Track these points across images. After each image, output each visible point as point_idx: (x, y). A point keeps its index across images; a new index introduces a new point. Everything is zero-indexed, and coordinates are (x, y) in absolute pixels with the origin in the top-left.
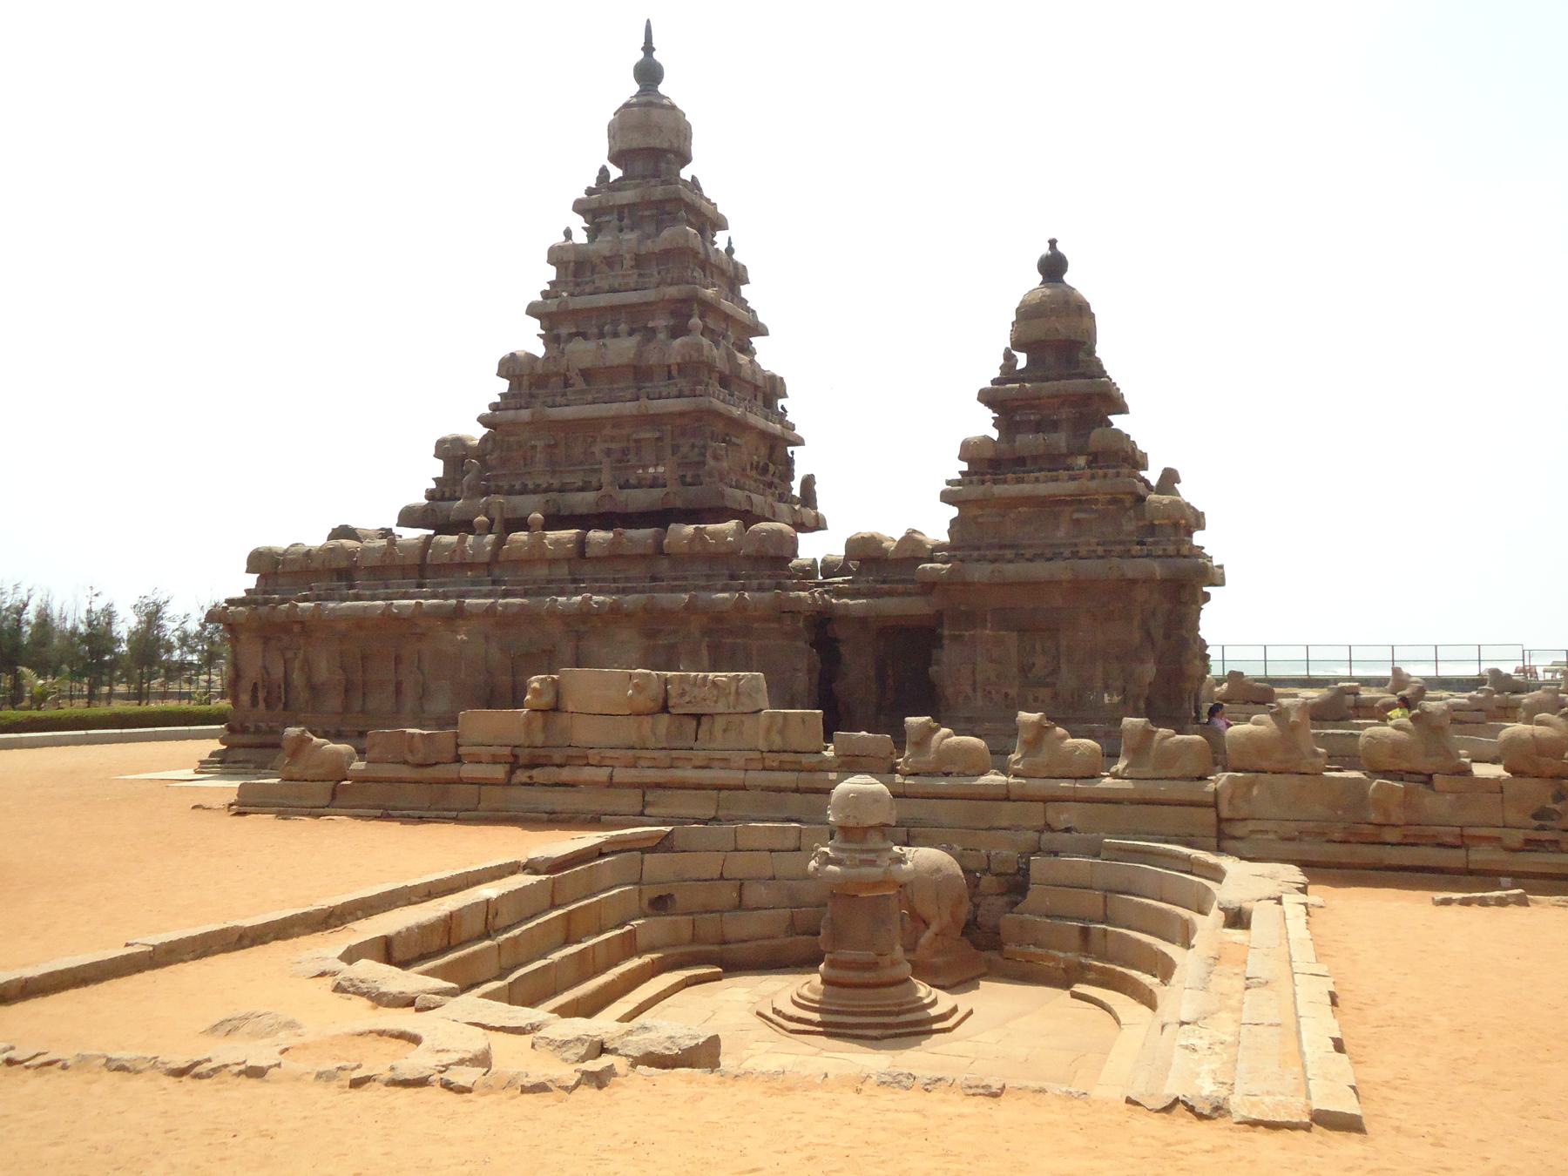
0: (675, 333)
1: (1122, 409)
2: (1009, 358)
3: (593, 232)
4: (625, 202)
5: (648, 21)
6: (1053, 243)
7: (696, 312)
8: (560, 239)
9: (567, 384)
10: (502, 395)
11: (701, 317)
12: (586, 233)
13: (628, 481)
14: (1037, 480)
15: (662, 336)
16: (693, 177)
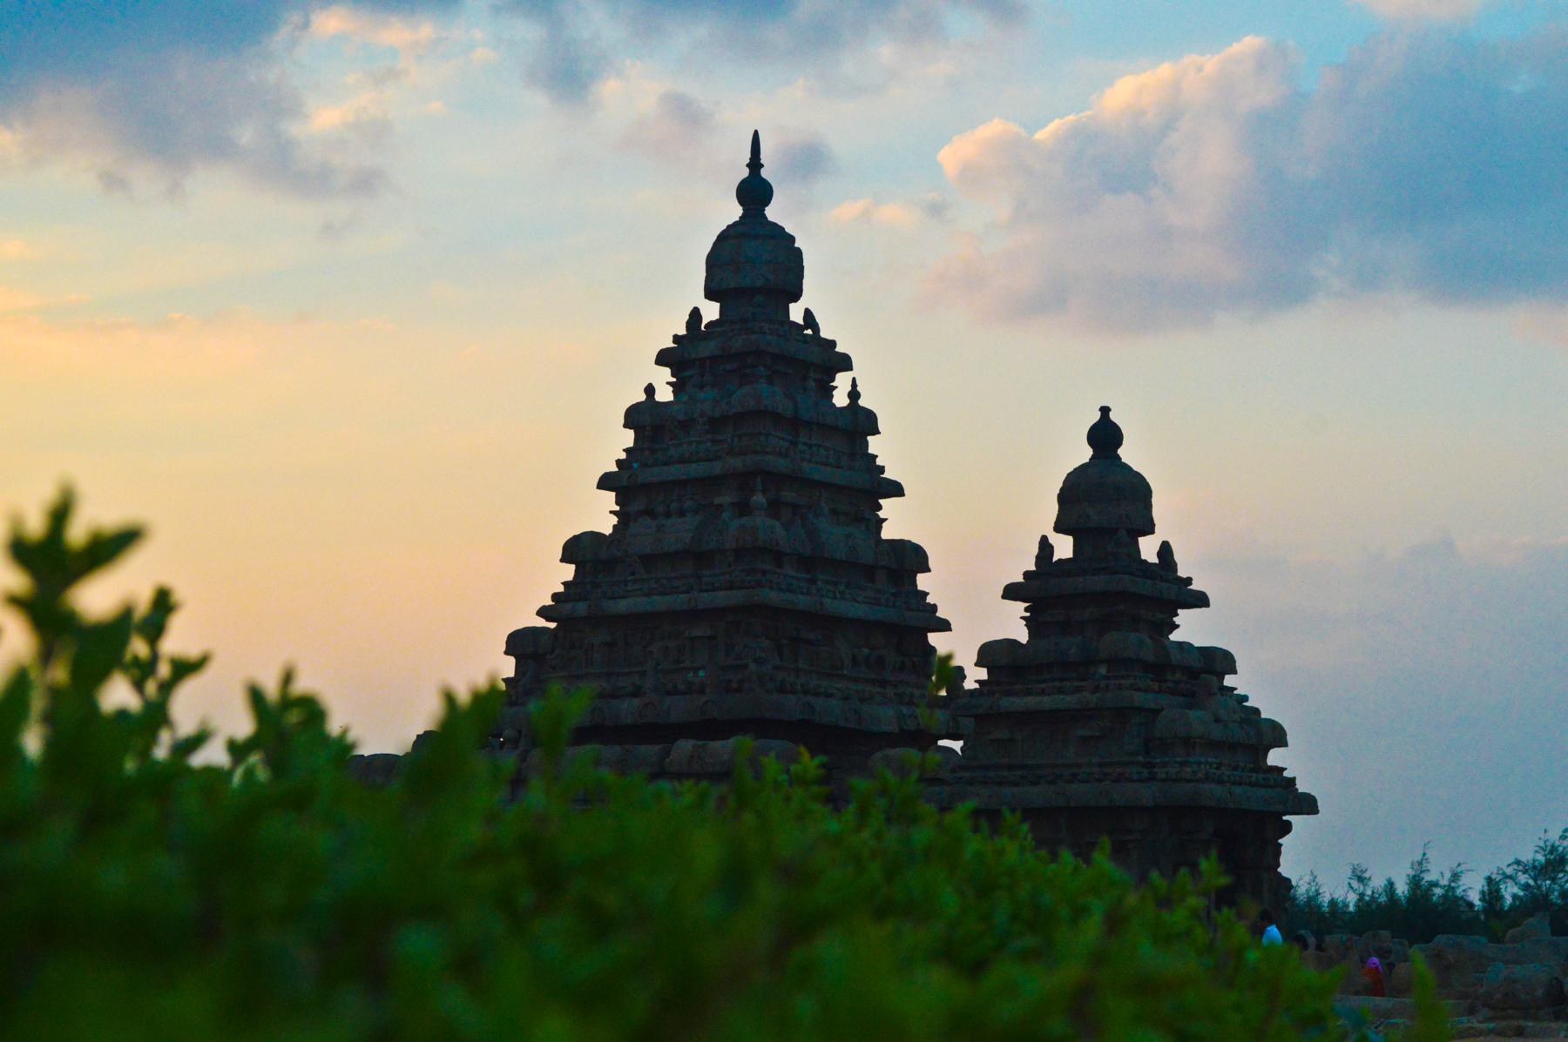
0: (743, 508)
1: (1201, 600)
2: (1045, 547)
3: (677, 387)
4: (707, 354)
5: (756, 134)
6: (1105, 411)
7: (760, 488)
8: (642, 397)
9: (633, 573)
10: (565, 584)
11: (764, 491)
12: (671, 389)
13: (676, 686)
14: (1043, 692)
15: (726, 515)
16: (808, 314)
